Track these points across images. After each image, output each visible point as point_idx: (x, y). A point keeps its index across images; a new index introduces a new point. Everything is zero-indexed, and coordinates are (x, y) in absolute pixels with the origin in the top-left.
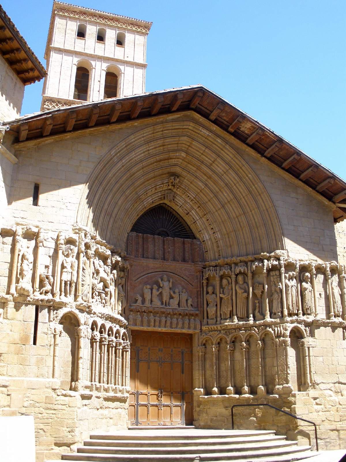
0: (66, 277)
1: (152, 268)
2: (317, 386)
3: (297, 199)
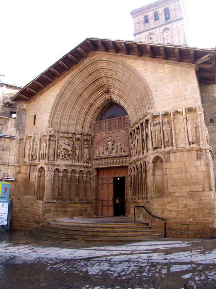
0: (41, 152)
1: (105, 137)
2: (173, 194)
3: (164, 72)
